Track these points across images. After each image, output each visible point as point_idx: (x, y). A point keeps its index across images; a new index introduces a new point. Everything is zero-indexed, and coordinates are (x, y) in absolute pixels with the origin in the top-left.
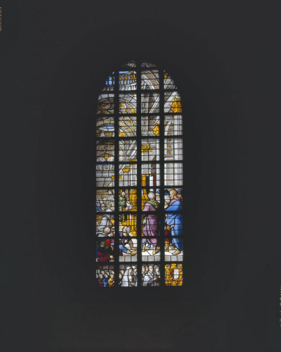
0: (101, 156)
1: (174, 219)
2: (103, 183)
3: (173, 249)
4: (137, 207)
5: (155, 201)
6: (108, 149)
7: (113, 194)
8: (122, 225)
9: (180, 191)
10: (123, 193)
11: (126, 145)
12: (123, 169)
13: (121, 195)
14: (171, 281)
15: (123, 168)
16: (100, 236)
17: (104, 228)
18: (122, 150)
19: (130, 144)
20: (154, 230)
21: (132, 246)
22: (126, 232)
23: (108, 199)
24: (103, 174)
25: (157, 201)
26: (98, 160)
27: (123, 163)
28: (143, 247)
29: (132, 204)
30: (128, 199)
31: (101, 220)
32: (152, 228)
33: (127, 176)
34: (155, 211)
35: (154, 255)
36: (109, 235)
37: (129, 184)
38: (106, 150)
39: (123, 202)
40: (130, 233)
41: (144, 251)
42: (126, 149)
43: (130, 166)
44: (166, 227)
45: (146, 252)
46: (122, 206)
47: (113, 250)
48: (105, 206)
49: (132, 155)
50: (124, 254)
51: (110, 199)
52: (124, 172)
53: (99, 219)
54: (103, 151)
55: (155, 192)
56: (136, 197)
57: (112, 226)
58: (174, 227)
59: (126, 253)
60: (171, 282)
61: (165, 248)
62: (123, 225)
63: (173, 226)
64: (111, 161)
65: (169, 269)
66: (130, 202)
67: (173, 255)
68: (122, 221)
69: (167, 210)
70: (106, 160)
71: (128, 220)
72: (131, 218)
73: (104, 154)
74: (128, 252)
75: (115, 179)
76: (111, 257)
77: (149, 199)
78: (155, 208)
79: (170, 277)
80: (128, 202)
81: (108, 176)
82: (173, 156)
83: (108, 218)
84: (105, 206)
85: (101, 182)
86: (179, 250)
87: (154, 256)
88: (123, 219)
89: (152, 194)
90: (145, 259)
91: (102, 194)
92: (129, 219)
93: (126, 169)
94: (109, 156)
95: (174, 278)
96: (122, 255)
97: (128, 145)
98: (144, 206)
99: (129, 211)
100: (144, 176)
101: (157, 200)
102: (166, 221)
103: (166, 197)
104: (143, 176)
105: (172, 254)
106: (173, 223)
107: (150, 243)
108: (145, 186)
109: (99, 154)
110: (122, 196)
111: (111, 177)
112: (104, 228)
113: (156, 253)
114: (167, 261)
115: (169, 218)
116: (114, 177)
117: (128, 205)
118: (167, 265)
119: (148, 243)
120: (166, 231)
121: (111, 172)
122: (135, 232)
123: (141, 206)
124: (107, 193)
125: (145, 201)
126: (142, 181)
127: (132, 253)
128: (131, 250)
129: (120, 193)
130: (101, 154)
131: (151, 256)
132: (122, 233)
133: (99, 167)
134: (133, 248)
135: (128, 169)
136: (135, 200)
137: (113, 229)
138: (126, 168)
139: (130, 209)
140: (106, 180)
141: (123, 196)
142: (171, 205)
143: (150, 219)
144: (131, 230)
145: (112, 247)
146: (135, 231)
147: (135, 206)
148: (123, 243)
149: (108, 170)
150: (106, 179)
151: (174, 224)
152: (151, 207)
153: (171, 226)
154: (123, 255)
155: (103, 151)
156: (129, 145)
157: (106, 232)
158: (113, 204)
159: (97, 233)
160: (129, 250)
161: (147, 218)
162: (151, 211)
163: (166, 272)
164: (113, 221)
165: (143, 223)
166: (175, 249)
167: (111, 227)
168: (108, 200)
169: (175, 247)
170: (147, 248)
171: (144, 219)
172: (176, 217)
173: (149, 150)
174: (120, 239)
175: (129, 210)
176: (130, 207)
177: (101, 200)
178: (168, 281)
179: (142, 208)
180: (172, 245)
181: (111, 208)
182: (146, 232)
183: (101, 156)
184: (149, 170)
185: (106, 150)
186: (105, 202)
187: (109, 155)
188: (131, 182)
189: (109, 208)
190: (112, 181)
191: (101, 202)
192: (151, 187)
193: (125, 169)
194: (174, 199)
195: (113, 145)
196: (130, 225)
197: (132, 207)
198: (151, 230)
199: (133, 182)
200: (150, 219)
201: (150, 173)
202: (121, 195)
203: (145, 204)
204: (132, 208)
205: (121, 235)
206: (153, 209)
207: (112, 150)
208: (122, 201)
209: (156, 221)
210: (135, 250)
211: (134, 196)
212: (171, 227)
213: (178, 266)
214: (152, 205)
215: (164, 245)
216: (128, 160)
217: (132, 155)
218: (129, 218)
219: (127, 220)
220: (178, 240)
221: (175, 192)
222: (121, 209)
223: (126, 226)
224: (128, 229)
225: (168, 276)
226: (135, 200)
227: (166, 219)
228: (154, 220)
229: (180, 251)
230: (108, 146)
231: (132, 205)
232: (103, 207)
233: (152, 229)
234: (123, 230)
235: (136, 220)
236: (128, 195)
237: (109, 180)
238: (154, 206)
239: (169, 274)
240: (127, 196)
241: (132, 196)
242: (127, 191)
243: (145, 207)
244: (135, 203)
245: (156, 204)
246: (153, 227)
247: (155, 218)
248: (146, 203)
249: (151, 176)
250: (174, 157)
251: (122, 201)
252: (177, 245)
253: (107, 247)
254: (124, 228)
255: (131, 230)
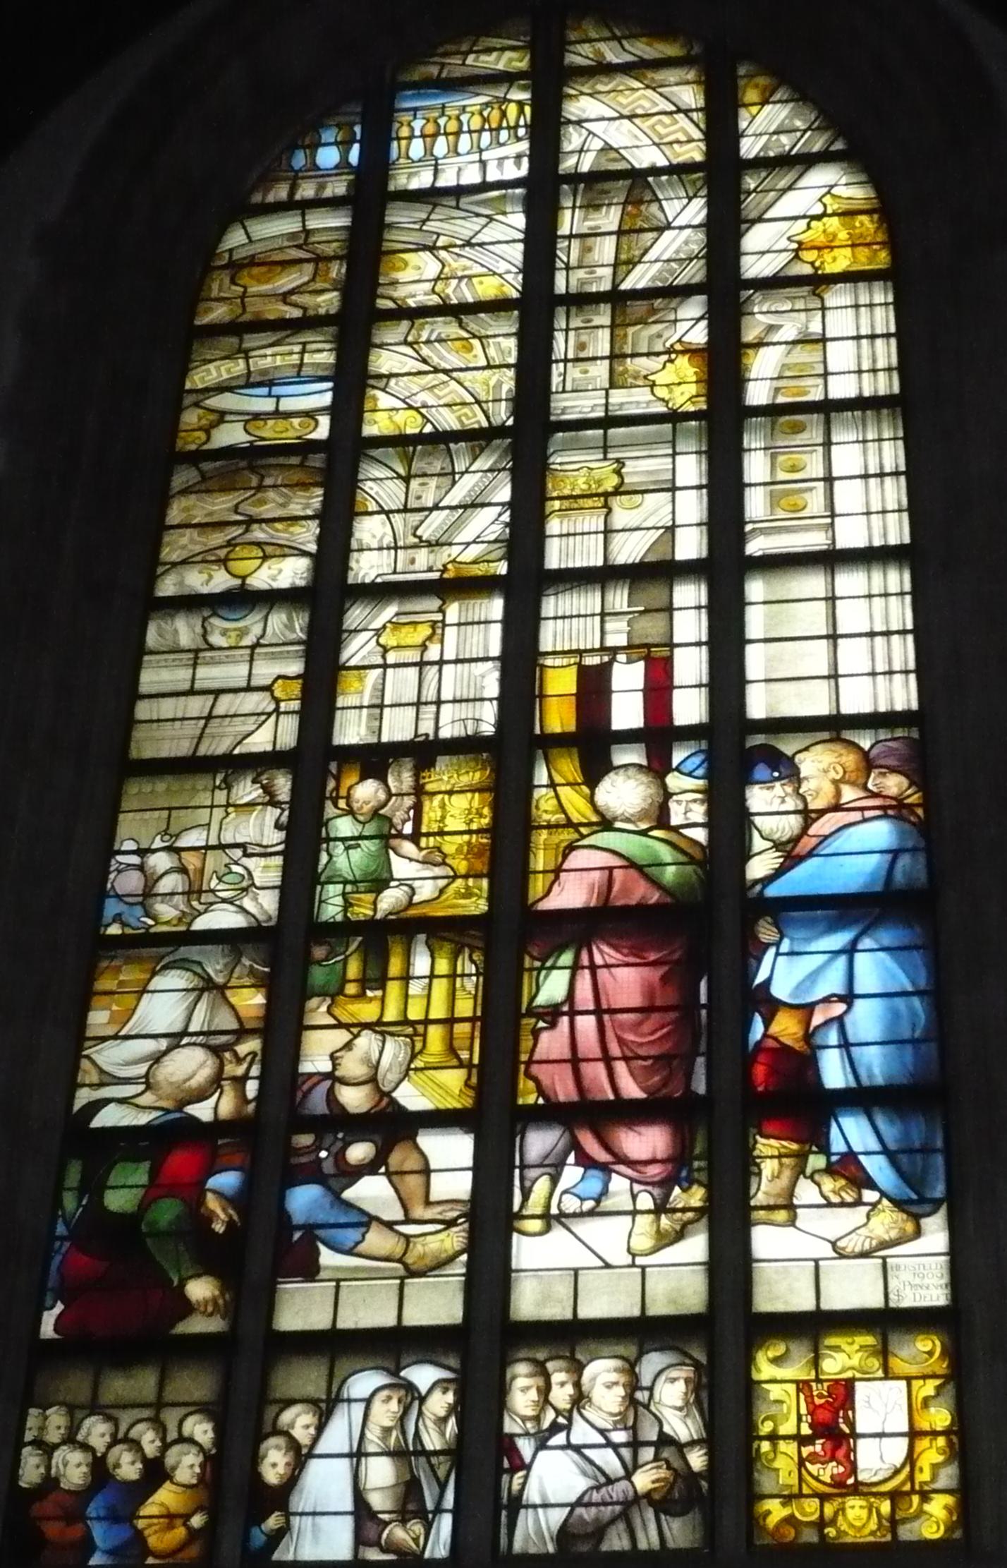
0: (199, 558)
1: (842, 961)
2: (193, 729)
3: (843, 1204)
4: (485, 883)
5: (656, 833)
6: (268, 511)
7: (274, 803)
8: (333, 1022)
9: (890, 753)
10: (367, 792)
11: (414, 484)
12: (378, 632)
13: (342, 804)
14: (823, 1498)
15: (377, 624)
16: (108, 1118)
17: (157, 1058)
18: (382, 511)
19: (451, 476)
20: (641, 1052)
21: (420, 1192)
22: (373, 1080)
23: (228, 838)
24: (202, 672)
25: (676, 829)
26: (167, 587)
27: (380, 592)
28: (526, 1194)
29: (444, 863)
30: (408, 829)
31: (144, 991)
32: (630, 1037)
33: (413, 671)
34: (657, 906)
35: (639, 1261)
36: (203, 1111)
37: (427, 727)
38: (251, 521)
39: (356, 855)
40: (405, 1084)
41: (535, 1225)
42: (413, 504)
43: (441, 610)
44: (767, 1023)
45: (558, 1232)
46: (345, 882)
47: (219, 1228)
48: (195, 891)
49: (466, 534)
50: (328, 1257)
51: (240, 840)
52: (385, 650)
53: (121, 984)
54: (222, 525)
55: (658, 767)
56: (486, 811)
57: (242, 1033)
58: (848, 1020)
59: (350, 1252)
60: (829, 1510)
61: (760, 1199)
62: (340, 1025)
63: (839, 1008)
64: (283, 583)
65: (802, 1386)
66: (421, 849)
67: (842, 1256)
68: (341, 991)
69: (772, 891)
70: (238, 582)
71: (394, 988)
72: (421, 964)
73: (230, 544)
74: (376, 1240)
75: (305, 697)
76: (200, 1289)
77: (606, 824)
78: (655, 883)
79: (813, 1458)
80: (408, 847)
81: (244, 684)
82: (829, 520)
83: (209, 980)
84: (195, 891)
85: (178, 724)
86: (899, 1204)
87: (643, 1268)
88: (344, 981)
89: (632, 783)
90: (546, 1298)
91: (170, 809)
92: (406, 978)
93: (405, 630)
94: (265, 558)
95: (853, 1469)
96: (310, 1271)
97: (433, 482)
98: (557, 871)
99: (412, 912)
100: (565, 662)
101: (675, 820)
102: (760, 979)
103: (759, 798)
104: (558, 662)
105: (834, 1244)
106: (832, 982)
107: (602, 1156)
108: (571, 727)
109: (184, 547)
110: (350, 812)
111: (268, 688)
112: (157, 1058)
113: (665, 1240)
114: (780, 1307)
115: (792, 953)
116: (296, 687)
117: (400, 868)
118: (778, 1349)
119: (586, 1161)
120: (762, 1058)
121: (273, 657)
122: (454, 1079)
123: (525, 873)
124: (221, 797)
125: (567, 836)
126: (542, 696)
127: (418, 1248)
128: (408, 1221)
129: (337, 788)
130: (198, 548)
131: (607, 1266)
132: (331, 1093)
133: (176, 631)
134: (428, 1203)
135: (425, 631)
136: (470, 832)
137: (239, 1060)
138: (404, 619)
139: (416, 899)
140: (221, 709)
141: (366, 808)
142: (811, 854)
143: (607, 966)
144: (413, 1056)
145: (212, 1203)
146: (461, 1065)
147: (466, 877)
148: (328, 1168)
149: (248, 641)
150: (225, 704)
151: (849, 997)
152: (617, 873)
153: (818, 1009)
154: (323, 1275)
155: (222, 525)
156: (446, 481)
157: (167, 1090)
158: (267, 872)
159: (83, 1097)
160: (390, 1225)
161: (577, 957)
162: (619, 903)
163: (762, 1411)
164: (251, 1001)
165: (541, 1000)
166: (858, 1202)
167: (228, 1047)
168: (222, 847)
169: (862, 1181)
170: (571, 1204)
171: (553, 967)
172: (866, 943)
173: (616, 502)
174: (305, 1140)
175: (410, 904)
176: (416, 884)
177: (158, 843)
178: (788, 1499)
179: (537, 885)
180: (830, 1170)
181: (247, 903)
182: (567, 1069)
183: (199, 558)
184: (610, 626)
185: (251, 521)
186: (191, 861)
187: (269, 550)
188: (446, 709)
189: (224, 901)
190: (277, 710)
191: (160, 862)
192: (628, 737)
193: (397, 626)
194: (837, 807)
195: (306, 490)
196: (406, 1022)
197: (442, 883)
198: (615, 1050)
199: (465, 710)
200: (607, 966)
201: (617, 638)
202: (342, 804)
203: (565, 857)
204: (442, 891)
205: (317, 1103)
206: (641, 892)
207: (295, 519)
208: (351, 842)
209: (664, 979)
210: (450, 1224)
211: (460, 803)
212: (817, 1019)
213: (891, 1348)
214: (631, 864)
215: (747, 1166)
216: (430, 570)
217: (466, 534)
218: (408, 963)
219: (383, 987)
220: (892, 1122)
221: (850, 759)
222: (339, 900)
223: (378, 1026)
224: (393, 1052)
225: (790, 1448)
226: (470, 832)
227: (759, 961)
228: (645, 971)
229: (916, 1218)
230: (271, 494)
231: (438, 871)
232: (172, 894)
233: (621, 1041)
234: (335, 1066)
235: (470, 984)
236: (409, 801)
237: (247, 708)
238: (653, 871)
239: (806, 1430)
240: (400, 811)
241: (443, 806)
242: (401, 778)
243: (563, 875)
244: (471, 852)
245: (666, 853)
246: (640, 1024)
247: (652, 957)
248: (571, 848)
249: (629, 662)
250: (832, 524)
251: (351, 842)
252: (877, 1167)
253: (167, 1212)
254: (348, 1046)
255: (413, 1056)
